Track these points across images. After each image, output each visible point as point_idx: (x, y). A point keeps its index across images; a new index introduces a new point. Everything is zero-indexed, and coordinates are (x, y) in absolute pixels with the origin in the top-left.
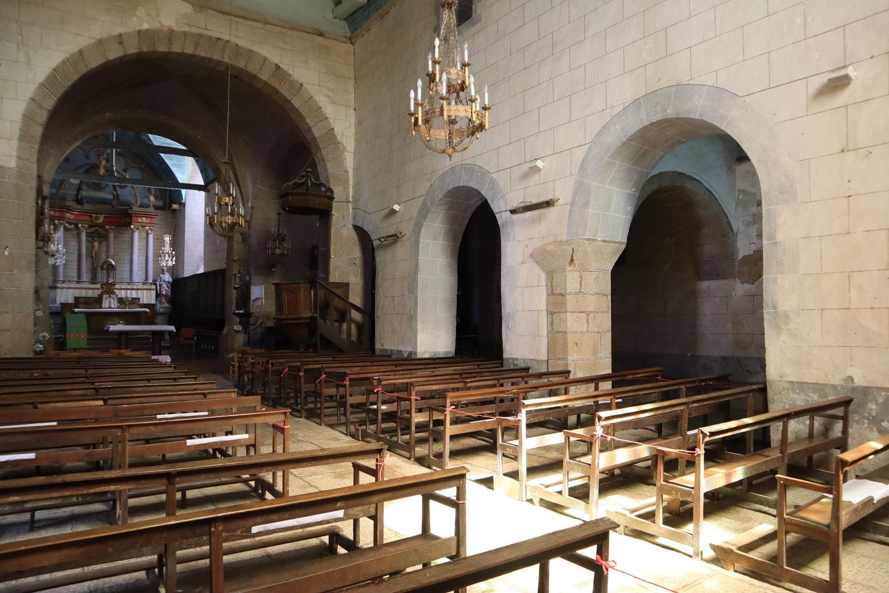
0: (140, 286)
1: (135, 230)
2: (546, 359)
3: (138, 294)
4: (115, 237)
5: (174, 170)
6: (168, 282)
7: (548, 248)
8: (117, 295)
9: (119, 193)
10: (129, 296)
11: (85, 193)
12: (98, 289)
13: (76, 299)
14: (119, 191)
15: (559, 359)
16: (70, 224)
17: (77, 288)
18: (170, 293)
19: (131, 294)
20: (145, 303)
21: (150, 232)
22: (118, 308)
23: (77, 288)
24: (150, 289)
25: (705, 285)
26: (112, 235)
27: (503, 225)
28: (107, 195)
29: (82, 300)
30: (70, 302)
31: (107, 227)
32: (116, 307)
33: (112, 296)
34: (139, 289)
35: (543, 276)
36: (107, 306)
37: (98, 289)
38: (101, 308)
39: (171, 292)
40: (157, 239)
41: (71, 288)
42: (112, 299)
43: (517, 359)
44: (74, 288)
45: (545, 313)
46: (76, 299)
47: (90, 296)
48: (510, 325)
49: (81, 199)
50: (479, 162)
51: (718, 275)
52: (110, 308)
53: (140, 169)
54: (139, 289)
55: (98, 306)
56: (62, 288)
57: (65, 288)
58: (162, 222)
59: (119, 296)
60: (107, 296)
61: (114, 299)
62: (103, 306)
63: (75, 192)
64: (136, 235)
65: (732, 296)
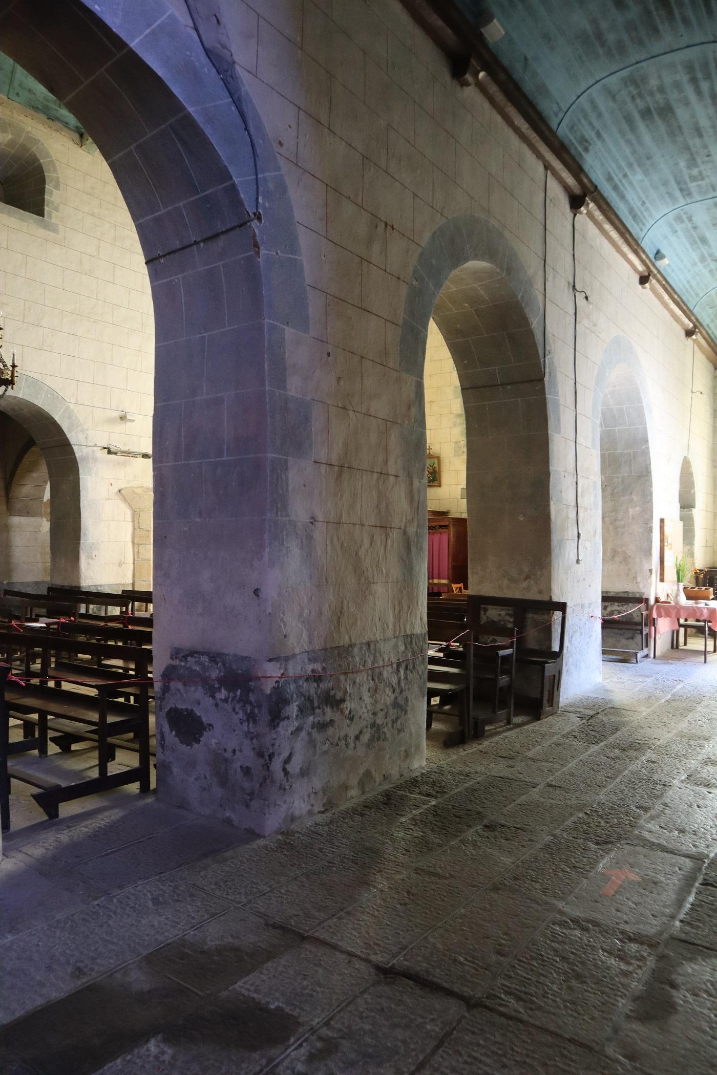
2: (131, 582)
7: (136, 490)
15: (144, 581)
25: (16, 520)
27: (85, 459)
35: (129, 513)
43: (101, 586)
45: (130, 544)
48: (94, 554)
50: (49, 382)
51: (28, 513)
65: (40, 531)
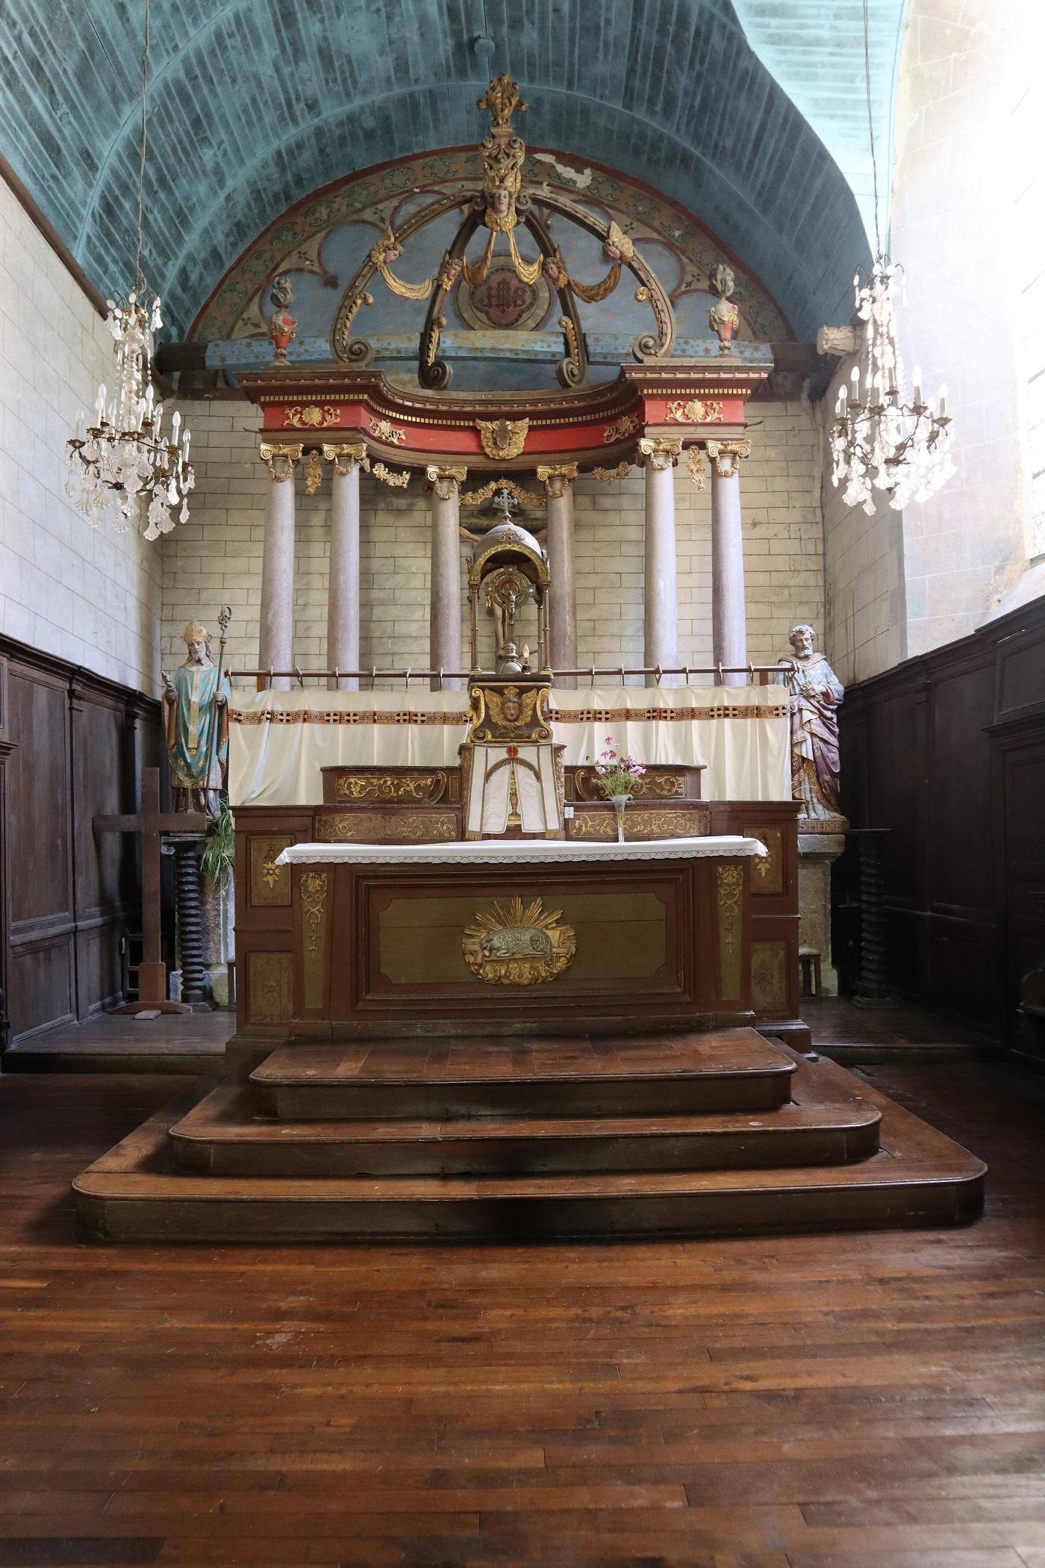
0: (701, 694)
1: (658, 461)
3: (685, 746)
4: (577, 526)
5: (826, 130)
6: (826, 695)
8: (558, 750)
9: (586, 326)
10: (636, 755)
11: (448, 341)
12: (458, 719)
13: (333, 775)
14: (589, 314)
16: (395, 468)
17: (341, 718)
18: (834, 756)
19: (647, 741)
20: (730, 796)
21: (725, 465)
22: (568, 831)
23: (341, 718)
24: (757, 712)
26: (563, 506)
28: (546, 343)
29: (356, 786)
30: (302, 800)
31: (543, 472)
32: (554, 824)
33: (526, 753)
34: (692, 714)
36: (497, 824)
37: (458, 719)
38: (462, 835)
39: (840, 738)
40: (754, 524)
41: (306, 717)
42: (521, 771)
44: (325, 718)
46: (333, 775)
47: (414, 758)
49: (439, 363)
52: (514, 832)
53: (669, 245)
54: (692, 714)
55: (444, 821)
56: (257, 718)
57: (272, 717)
58: (772, 453)
59: (567, 759)
60: (499, 754)
61: (538, 777)
62: (473, 825)
63: (416, 343)
64: (665, 482)
